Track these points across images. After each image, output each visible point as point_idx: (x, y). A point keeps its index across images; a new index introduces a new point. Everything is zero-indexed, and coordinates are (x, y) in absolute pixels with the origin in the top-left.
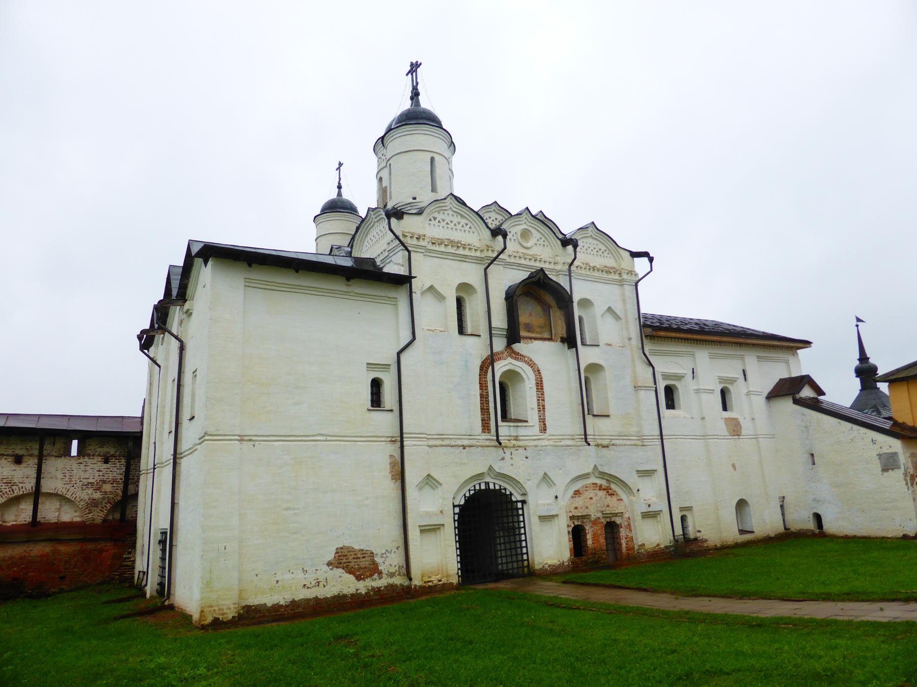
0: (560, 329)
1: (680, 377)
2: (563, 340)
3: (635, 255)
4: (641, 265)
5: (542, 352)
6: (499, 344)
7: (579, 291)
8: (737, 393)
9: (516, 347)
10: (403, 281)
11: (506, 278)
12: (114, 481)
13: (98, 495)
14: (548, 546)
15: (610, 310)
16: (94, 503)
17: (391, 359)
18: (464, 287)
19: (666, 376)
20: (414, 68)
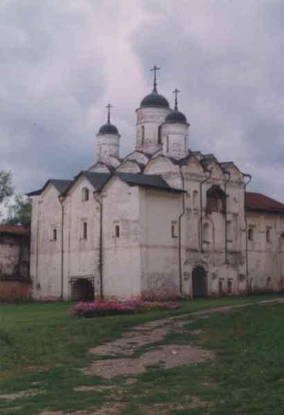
0: (220, 205)
1: (254, 226)
2: (221, 212)
3: (244, 175)
4: (246, 179)
5: (216, 218)
6: (204, 214)
7: (228, 191)
8: (272, 232)
9: (209, 215)
10: (179, 193)
11: (206, 187)
12: (14, 256)
13: (9, 262)
14: (213, 286)
15: (235, 199)
16: (8, 266)
17: (177, 219)
18: (195, 191)
19: (250, 226)
20: (176, 91)
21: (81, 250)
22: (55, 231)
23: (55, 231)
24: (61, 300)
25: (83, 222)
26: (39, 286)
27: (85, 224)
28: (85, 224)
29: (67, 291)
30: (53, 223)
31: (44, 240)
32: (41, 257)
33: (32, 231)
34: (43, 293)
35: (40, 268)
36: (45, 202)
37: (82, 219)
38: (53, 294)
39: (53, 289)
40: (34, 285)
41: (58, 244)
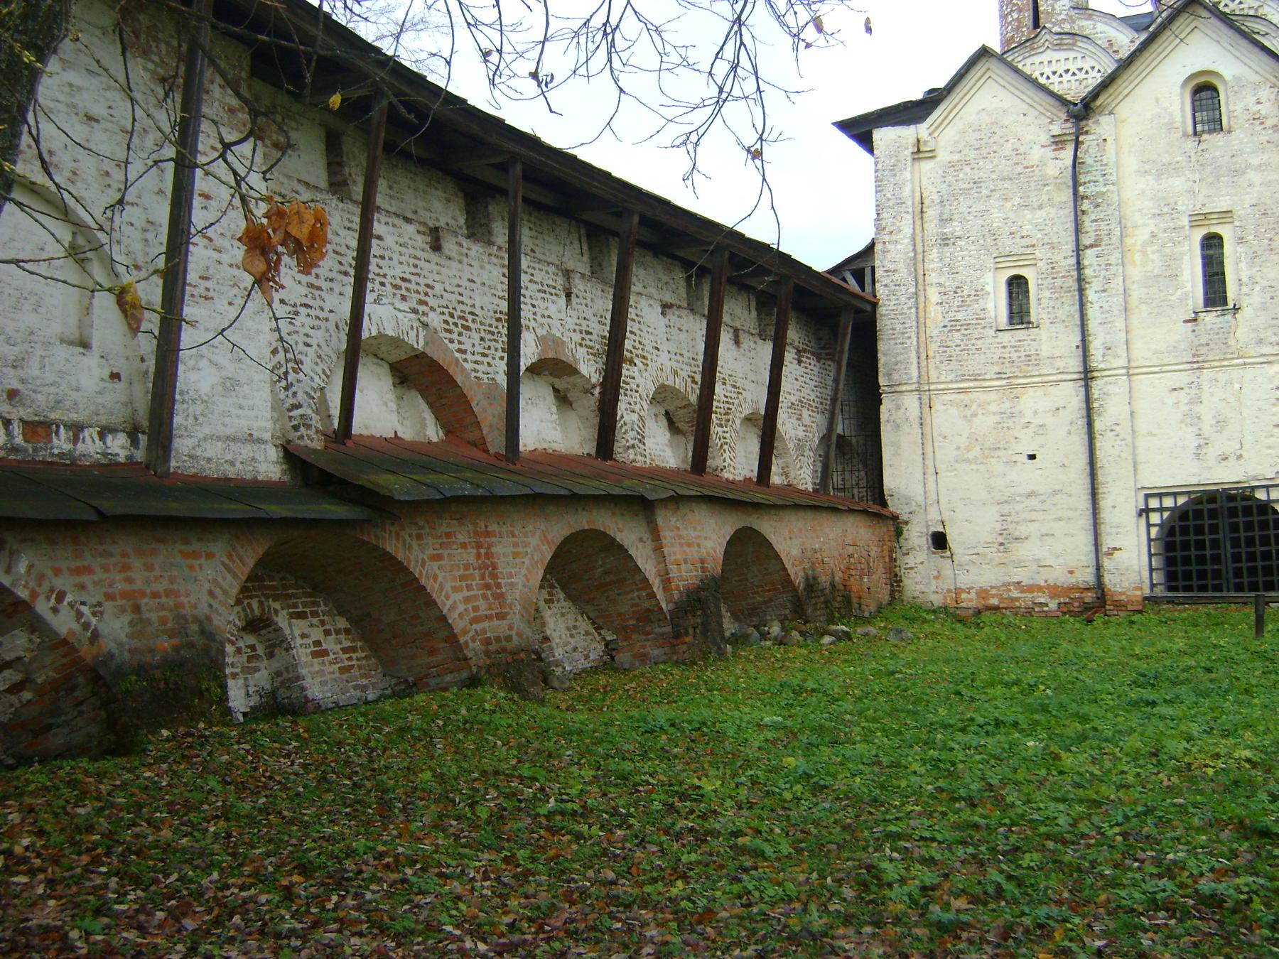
21: (1197, 363)
22: (1017, 285)
23: (1017, 285)
24: (1094, 603)
25: (1199, 234)
26: (939, 541)
27: (1212, 243)
28: (1212, 243)
29: (1132, 562)
30: (1006, 244)
31: (954, 326)
32: (946, 416)
33: (881, 291)
34: (974, 572)
35: (945, 454)
36: (943, 156)
37: (1198, 219)
38: (1024, 576)
39: (1024, 551)
40: (916, 536)
41: (1052, 339)
